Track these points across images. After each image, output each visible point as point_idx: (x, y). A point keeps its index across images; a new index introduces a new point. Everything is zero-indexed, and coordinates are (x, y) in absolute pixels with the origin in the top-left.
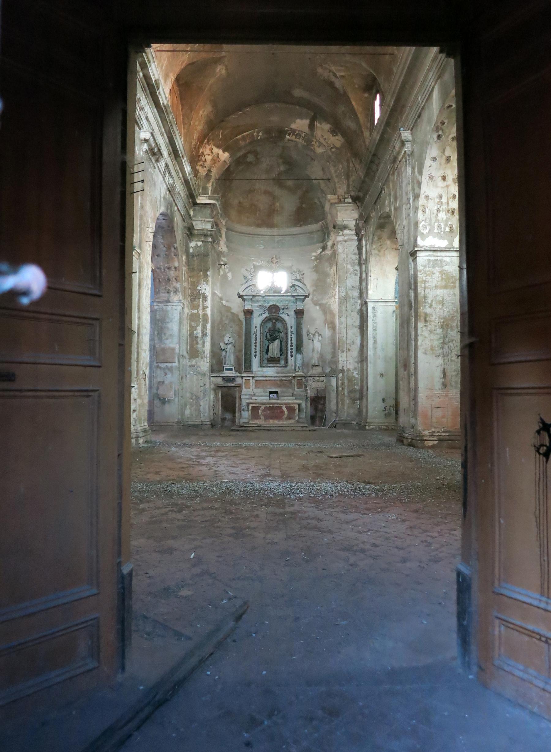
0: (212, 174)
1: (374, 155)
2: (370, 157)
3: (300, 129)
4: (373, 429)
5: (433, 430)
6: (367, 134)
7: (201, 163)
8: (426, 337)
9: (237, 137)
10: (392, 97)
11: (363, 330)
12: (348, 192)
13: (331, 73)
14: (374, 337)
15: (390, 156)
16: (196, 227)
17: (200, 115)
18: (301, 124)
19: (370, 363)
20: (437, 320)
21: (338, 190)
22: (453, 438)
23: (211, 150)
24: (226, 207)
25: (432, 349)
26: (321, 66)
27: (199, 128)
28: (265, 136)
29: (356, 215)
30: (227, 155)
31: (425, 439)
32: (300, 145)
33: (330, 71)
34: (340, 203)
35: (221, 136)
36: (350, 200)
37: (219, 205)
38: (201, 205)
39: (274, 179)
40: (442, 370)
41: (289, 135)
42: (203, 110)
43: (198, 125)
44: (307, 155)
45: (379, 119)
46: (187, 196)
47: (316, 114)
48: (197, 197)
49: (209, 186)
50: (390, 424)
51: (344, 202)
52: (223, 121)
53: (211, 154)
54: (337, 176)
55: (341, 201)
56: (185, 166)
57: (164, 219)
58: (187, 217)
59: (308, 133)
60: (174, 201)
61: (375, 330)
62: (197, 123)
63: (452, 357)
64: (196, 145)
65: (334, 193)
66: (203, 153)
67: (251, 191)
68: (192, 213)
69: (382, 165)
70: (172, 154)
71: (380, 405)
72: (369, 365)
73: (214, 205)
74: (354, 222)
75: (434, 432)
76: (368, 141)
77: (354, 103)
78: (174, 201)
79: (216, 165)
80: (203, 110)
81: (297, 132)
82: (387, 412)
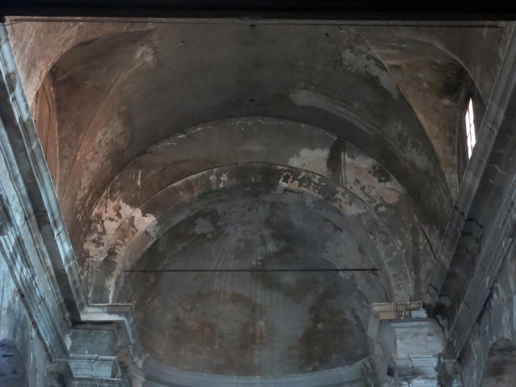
0: (118, 260)
1: (470, 219)
2: (463, 224)
3: (310, 169)
6: (452, 177)
7: (95, 236)
9: (175, 185)
10: (500, 106)
12: (417, 296)
13: (372, 62)
15: (505, 222)
16: (78, 374)
17: (97, 140)
18: (311, 159)
21: (396, 292)
23: (117, 210)
24: (145, 328)
26: (351, 48)
27: (94, 166)
28: (235, 182)
29: (439, 347)
30: (150, 220)
32: (309, 201)
33: (369, 58)
34: (403, 321)
35: (139, 183)
36: (423, 314)
37: (131, 325)
38: (89, 326)
39: (252, 270)
41: (286, 180)
42: (103, 130)
43: (91, 161)
44: (326, 220)
45: (475, 150)
46: (60, 305)
47: (342, 140)
48: (82, 306)
49: (111, 284)
51: (409, 318)
52: (144, 152)
53: (116, 218)
54: (390, 264)
55: (403, 316)
56: (58, 243)
57: (5, 356)
58: (57, 352)
59: (325, 175)
60: (31, 316)
62: (88, 157)
64: (84, 200)
65: (388, 298)
66: (99, 216)
67: (201, 296)
68: (68, 343)
69: (488, 240)
70: (33, 218)
73: (119, 325)
74: (434, 362)
76: (454, 192)
77: (421, 117)
78: (31, 316)
79: (126, 240)
80: (103, 130)
81: (303, 174)
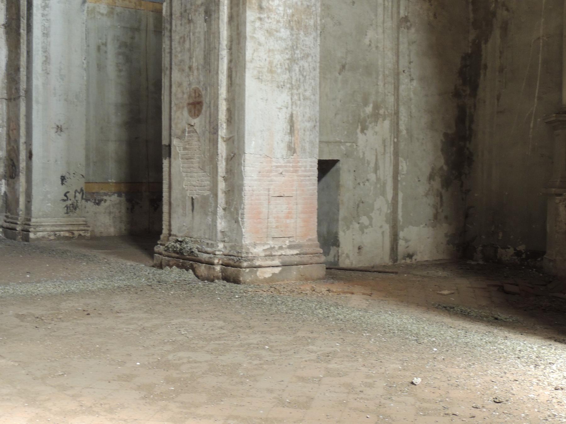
4: (43, 237)
5: (271, 243)
8: (260, 44)
11: (19, 34)
14: (45, 51)
19: (38, 102)
20: (281, 8)
22: (306, 258)
25: (271, 71)
31: (258, 263)
40: (288, 116)
50: (76, 228)
61: (46, 34)
63: (305, 90)
71: (57, 190)
72: (35, 106)
75: (272, 248)
82: (69, 202)
